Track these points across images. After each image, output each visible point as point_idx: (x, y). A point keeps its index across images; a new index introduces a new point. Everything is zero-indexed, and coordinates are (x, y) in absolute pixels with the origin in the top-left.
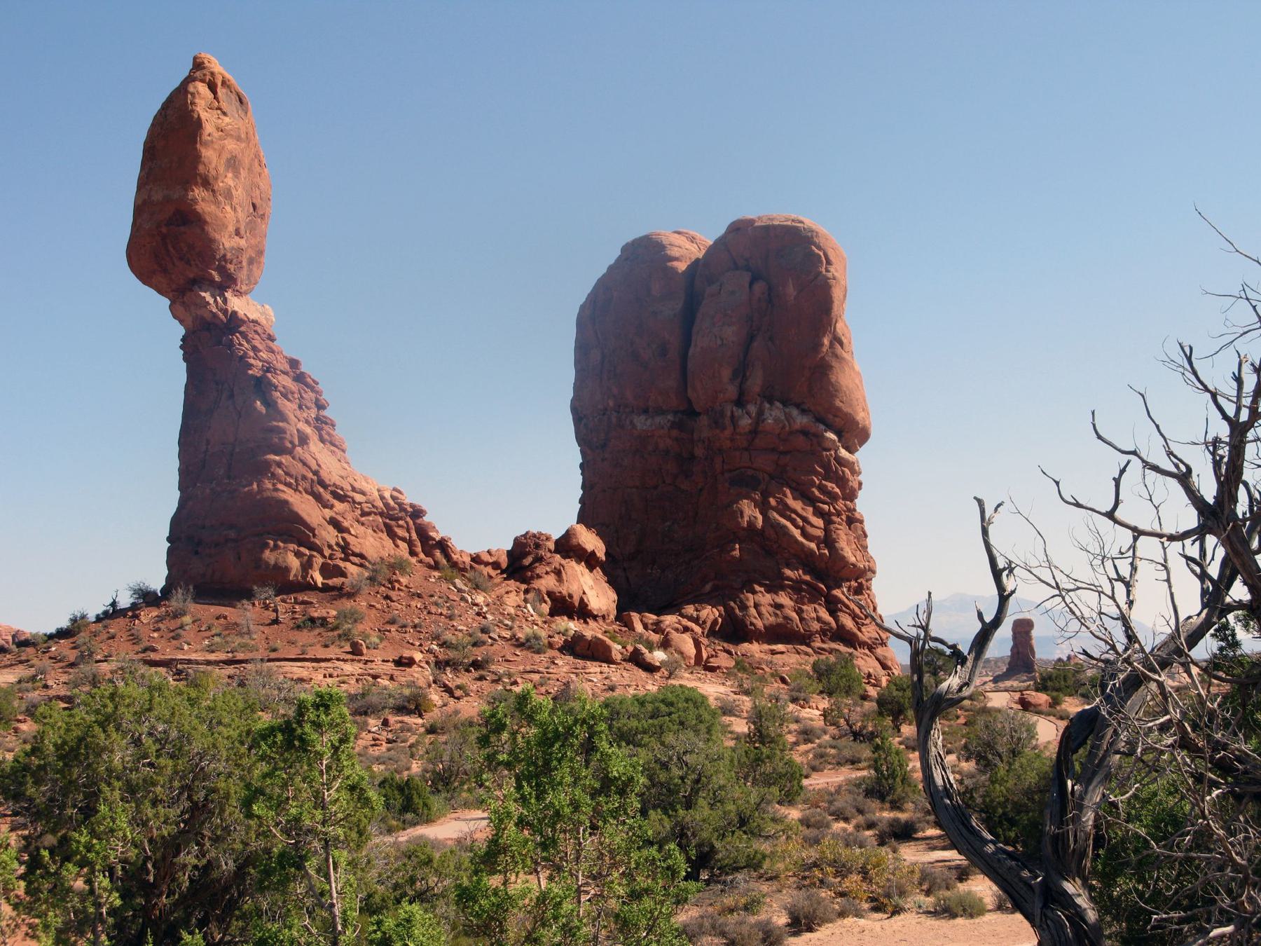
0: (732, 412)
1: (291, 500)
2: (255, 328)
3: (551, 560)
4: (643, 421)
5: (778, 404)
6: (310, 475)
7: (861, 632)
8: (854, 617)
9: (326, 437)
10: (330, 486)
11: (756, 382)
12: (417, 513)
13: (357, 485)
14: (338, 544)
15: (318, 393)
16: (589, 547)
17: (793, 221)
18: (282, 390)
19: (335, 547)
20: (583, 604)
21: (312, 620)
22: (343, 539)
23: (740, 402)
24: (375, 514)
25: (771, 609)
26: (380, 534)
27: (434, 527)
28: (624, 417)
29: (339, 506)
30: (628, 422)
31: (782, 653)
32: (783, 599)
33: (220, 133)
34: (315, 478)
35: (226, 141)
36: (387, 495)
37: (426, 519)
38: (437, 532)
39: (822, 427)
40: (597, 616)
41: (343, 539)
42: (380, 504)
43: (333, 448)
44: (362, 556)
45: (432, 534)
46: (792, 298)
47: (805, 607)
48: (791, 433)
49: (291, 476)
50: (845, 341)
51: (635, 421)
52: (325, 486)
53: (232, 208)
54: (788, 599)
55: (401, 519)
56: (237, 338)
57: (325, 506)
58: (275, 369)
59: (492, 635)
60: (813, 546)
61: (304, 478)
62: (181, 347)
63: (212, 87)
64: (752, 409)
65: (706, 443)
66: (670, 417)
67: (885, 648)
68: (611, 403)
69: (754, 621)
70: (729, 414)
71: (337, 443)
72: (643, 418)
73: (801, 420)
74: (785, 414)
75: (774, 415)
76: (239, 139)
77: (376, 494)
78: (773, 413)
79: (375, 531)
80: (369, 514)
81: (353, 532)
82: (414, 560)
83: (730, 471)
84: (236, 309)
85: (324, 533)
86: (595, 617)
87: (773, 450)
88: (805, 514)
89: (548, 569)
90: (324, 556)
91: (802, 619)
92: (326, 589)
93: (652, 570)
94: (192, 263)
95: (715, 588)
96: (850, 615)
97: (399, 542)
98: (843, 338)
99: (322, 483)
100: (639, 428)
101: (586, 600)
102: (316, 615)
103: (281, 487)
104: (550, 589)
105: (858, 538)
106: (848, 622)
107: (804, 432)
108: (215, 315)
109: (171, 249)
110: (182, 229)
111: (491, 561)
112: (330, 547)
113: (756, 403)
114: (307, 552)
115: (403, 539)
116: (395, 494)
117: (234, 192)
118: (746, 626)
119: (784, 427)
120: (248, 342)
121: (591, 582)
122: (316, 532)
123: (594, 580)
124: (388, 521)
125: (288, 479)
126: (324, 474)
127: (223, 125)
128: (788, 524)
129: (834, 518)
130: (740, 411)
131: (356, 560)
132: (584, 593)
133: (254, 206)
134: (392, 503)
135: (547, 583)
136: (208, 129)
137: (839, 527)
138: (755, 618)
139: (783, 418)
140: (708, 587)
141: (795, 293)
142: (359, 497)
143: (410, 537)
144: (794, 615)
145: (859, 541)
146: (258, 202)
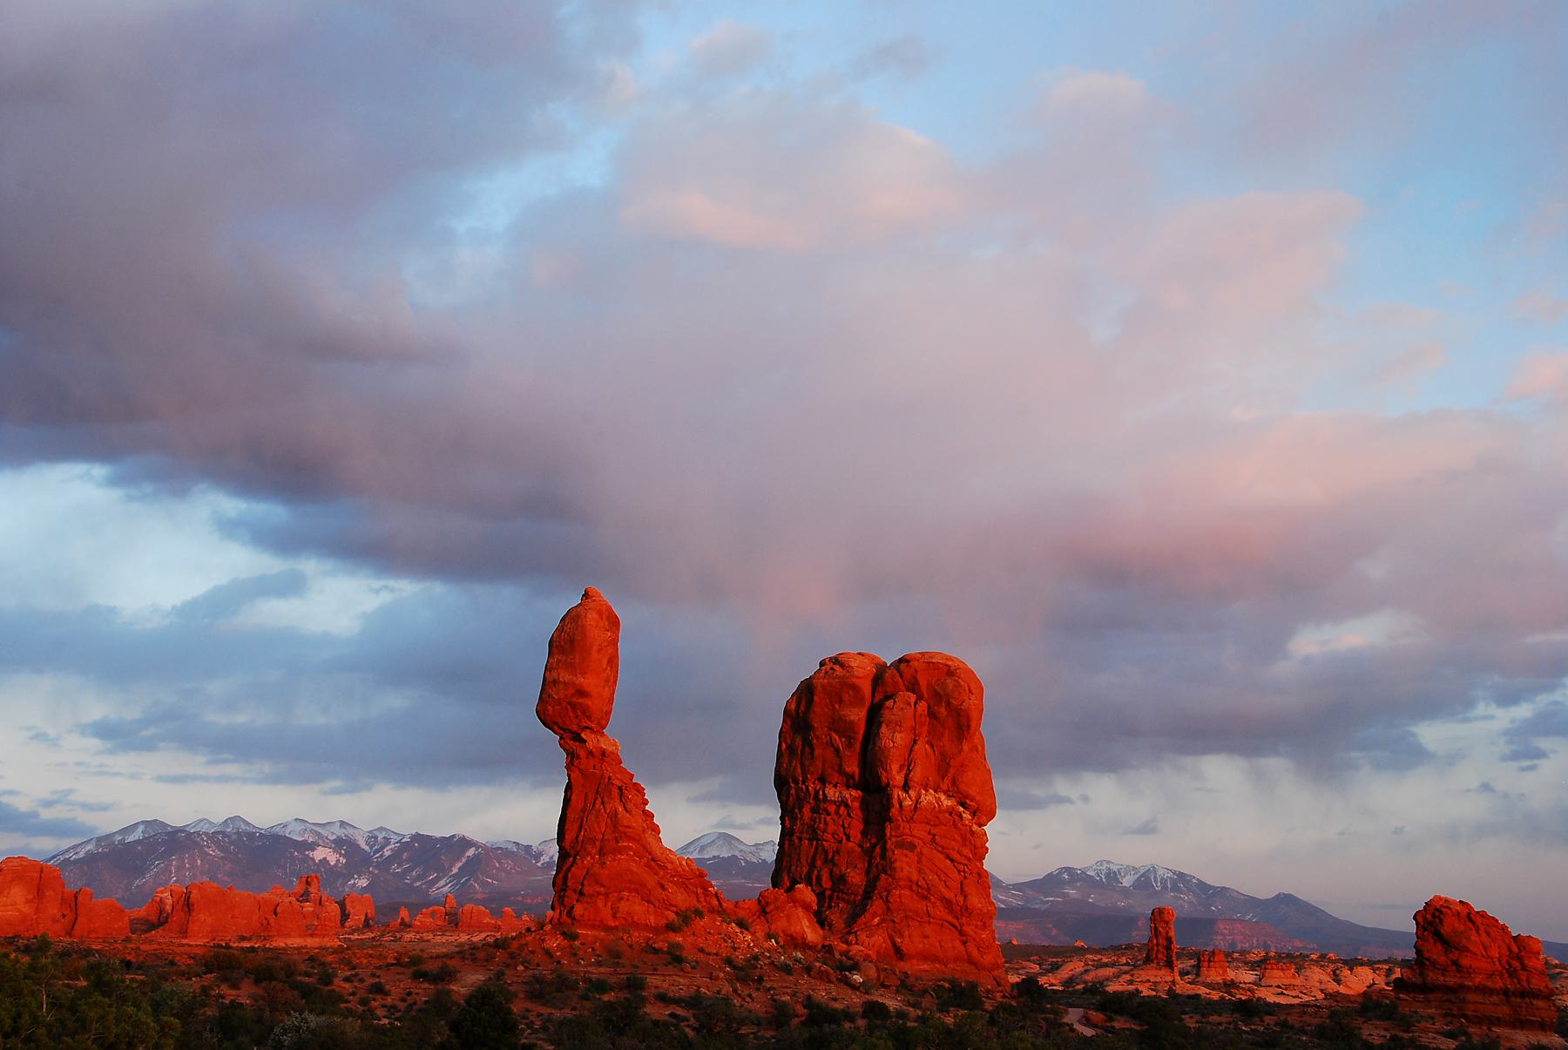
11: (917, 774)
20: (804, 939)
22: (667, 896)
30: (821, 793)
31: (927, 971)
32: (928, 929)
34: (650, 857)
39: (962, 809)
44: (675, 906)
48: (940, 812)
51: (826, 792)
60: (949, 895)
64: (912, 793)
70: (896, 796)
73: (947, 803)
75: (928, 798)
78: (927, 798)
80: (675, 876)
90: (655, 906)
95: (883, 921)
99: (653, 859)
106: (975, 952)
107: (951, 811)
110: (580, 700)
121: (807, 924)
131: (674, 909)
140: (876, 920)
144: (938, 944)
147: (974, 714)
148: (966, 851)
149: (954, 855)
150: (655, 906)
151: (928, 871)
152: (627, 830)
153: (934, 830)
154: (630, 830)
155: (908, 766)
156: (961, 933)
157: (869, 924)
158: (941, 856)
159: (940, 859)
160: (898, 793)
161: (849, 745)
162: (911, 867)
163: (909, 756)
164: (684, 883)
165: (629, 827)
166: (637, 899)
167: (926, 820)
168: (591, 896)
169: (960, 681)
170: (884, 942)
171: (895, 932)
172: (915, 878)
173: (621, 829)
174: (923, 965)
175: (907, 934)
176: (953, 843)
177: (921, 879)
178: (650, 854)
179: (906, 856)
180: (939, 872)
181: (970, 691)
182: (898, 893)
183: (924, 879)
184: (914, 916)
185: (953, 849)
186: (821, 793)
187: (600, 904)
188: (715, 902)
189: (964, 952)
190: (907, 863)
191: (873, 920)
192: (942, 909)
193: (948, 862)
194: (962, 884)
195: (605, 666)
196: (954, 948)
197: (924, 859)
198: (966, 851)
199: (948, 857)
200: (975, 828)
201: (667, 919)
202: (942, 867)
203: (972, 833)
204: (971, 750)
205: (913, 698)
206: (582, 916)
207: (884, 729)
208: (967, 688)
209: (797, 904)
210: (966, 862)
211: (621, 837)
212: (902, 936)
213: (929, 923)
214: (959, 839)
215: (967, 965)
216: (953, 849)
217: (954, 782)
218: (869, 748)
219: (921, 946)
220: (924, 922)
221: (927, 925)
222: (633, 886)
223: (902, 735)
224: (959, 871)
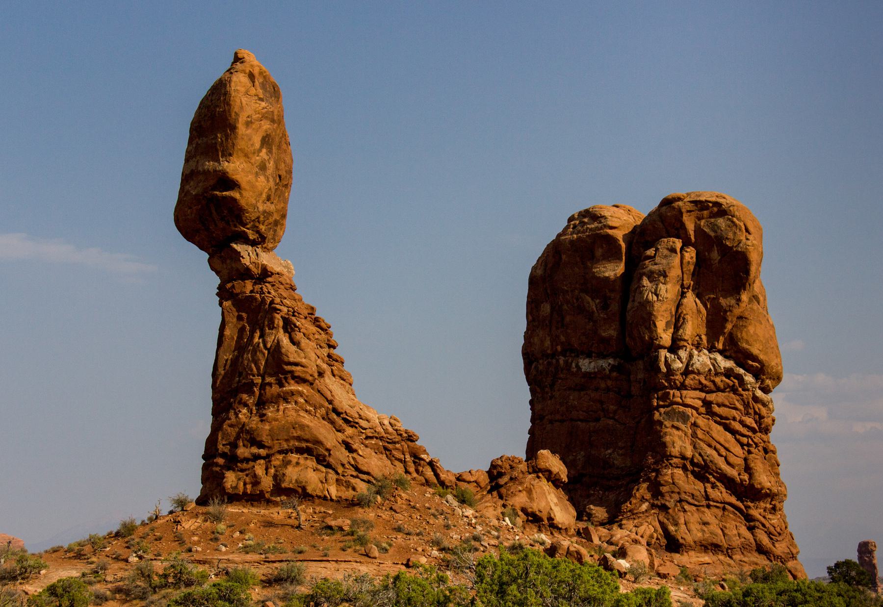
0: (666, 357)
1: (311, 424)
2: (280, 279)
3: (523, 480)
4: (586, 364)
5: (705, 351)
6: (326, 404)
7: (775, 546)
8: (769, 534)
9: (336, 372)
10: (342, 413)
12: (411, 438)
13: (362, 413)
14: (349, 463)
15: (331, 335)
16: (555, 470)
17: (717, 196)
18: (305, 331)
19: (347, 466)
20: (550, 519)
21: (330, 528)
22: (354, 459)
23: (674, 349)
24: (377, 438)
25: (699, 527)
26: (381, 456)
27: (425, 451)
28: (570, 361)
29: (349, 431)
30: (574, 365)
33: (257, 115)
34: (330, 407)
35: (262, 122)
36: (386, 422)
37: (418, 443)
38: (428, 454)
39: (742, 371)
40: (561, 529)
41: (354, 459)
42: (380, 429)
43: (342, 382)
44: (368, 473)
45: (423, 456)
46: (717, 261)
47: (728, 525)
49: (310, 405)
50: (761, 299)
51: (580, 364)
52: (338, 414)
53: (265, 178)
54: (714, 518)
55: (398, 442)
56: (265, 286)
57: (339, 431)
58: (299, 314)
59: (482, 543)
61: (322, 406)
62: (217, 294)
63: (251, 76)
64: (683, 354)
65: (642, 384)
66: (611, 361)
67: (795, 561)
68: (559, 348)
69: (684, 536)
70: (663, 359)
71: (345, 378)
72: (587, 361)
73: (724, 363)
74: (710, 358)
75: (702, 360)
76: (273, 121)
77: (377, 421)
78: (701, 359)
79: (376, 453)
80: (371, 438)
81: (361, 453)
82: (409, 477)
83: (663, 407)
84: (265, 262)
85: (337, 453)
86: (559, 529)
87: (701, 390)
88: (727, 445)
89: (520, 488)
90: (337, 473)
91: (724, 535)
92: (339, 501)
93: (594, 491)
94: (231, 223)
96: (766, 532)
97: (397, 463)
98: (760, 296)
99: (335, 410)
100: (583, 370)
101: (552, 515)
102: (333, 523)
103: (302, 413)
104: (522, 505)
105: (772, 466)
106: (765, 540)
107: (728, 373)
108: (248, 269)
109: (214, 212)
111: (472, 480)
112: (343, 465)
113: (686, 350)
114: (323, 469)
115: (400, 460)
116: (392, 421)
117: (267, 164)
118: (678, 540)
119: (710, 370)
120: (276, 291)
121: (555, 500)
122: (331, 452)
123: (558, 499)
124: (386, 444)
125: (308, 408)
126: (336, 403)
127: (260, 108)
128: (714, 453)
129: (752, 449)
130: (673, 356)
131: (365, 477)
132: (551, 509)
133: (280, 177)
134: (390, 429)
135: (520, 500)
136: (248, 111)
137: (757, 457)
138: (686, 533)
139: (709, 363)
140: (645, 506)
141: (719, 258)
142: (363, 423)
143: (405, 458)
144: (720, 532)
145: (772, 469)
146: (283, 173)
147: (753, 257)
148: (749, 421)
149: (737, 426)
150: (337, 473)
151: (705, 446)
152: (294, 368)
153: (711, 397)
154: (299, 368)
155: (678, 322)
156: (749, 518)
157: (635, 512)
158: (720, 428)
159: (718, 432)
160: (663, 353)
161: (605, 307)
162: (684, 442)
163: (677, 311)
164: (386, 448)
165: (296, 364)
166: (312, 463)
167: (700, 387)
168: (247, 460)
169: (735, 219)
170: (656, 531)
171: (668, 520)
172: (689, 453)
173: (288, 368)
174: (704, 556)
175: (682, 521)
176: (734, 411)
177: (697, 455)
178: (330, 402)
179: (678, 429)
180: (718, 446)
181: (747, 230)
182: (670, 472)
183: (700, 454)
184: (690, 500)
185: (734, 419)
186: (574, 365)
187: (259, 470)
188: (429, 473)
189: (752, 541)
190: (680, 437)
191: (640, 506)
192: (724, 490)
193: (729, 435)
194: (746, 459)
195: (257, 145)
196: (739, 535)
197: (700, 433)
198: (749, 421)
199: (727, 428)
200: (759, 393)
201: (354, 489)
202: (722, 441)
203: (756, 399)
204: (750, 301)
205: (678, 244)
206: (236, 487)
207: (645, 282)
208: (743, 227)
209: (540, 475)
210: (750, 434)
211: (286, 379)
212: (676, 524)
213: (708, 506)
214: (741, 407)
215: (756, 554)
216: (734, 419)
217: (732, 340)
218: (629, 306)
219: (700, 535)
220: (703, 506)
221: (706, 510)
222: (304, 445)
223: (669, 286)
224: (742, 445)
